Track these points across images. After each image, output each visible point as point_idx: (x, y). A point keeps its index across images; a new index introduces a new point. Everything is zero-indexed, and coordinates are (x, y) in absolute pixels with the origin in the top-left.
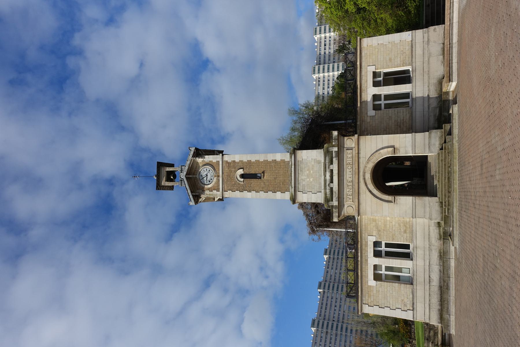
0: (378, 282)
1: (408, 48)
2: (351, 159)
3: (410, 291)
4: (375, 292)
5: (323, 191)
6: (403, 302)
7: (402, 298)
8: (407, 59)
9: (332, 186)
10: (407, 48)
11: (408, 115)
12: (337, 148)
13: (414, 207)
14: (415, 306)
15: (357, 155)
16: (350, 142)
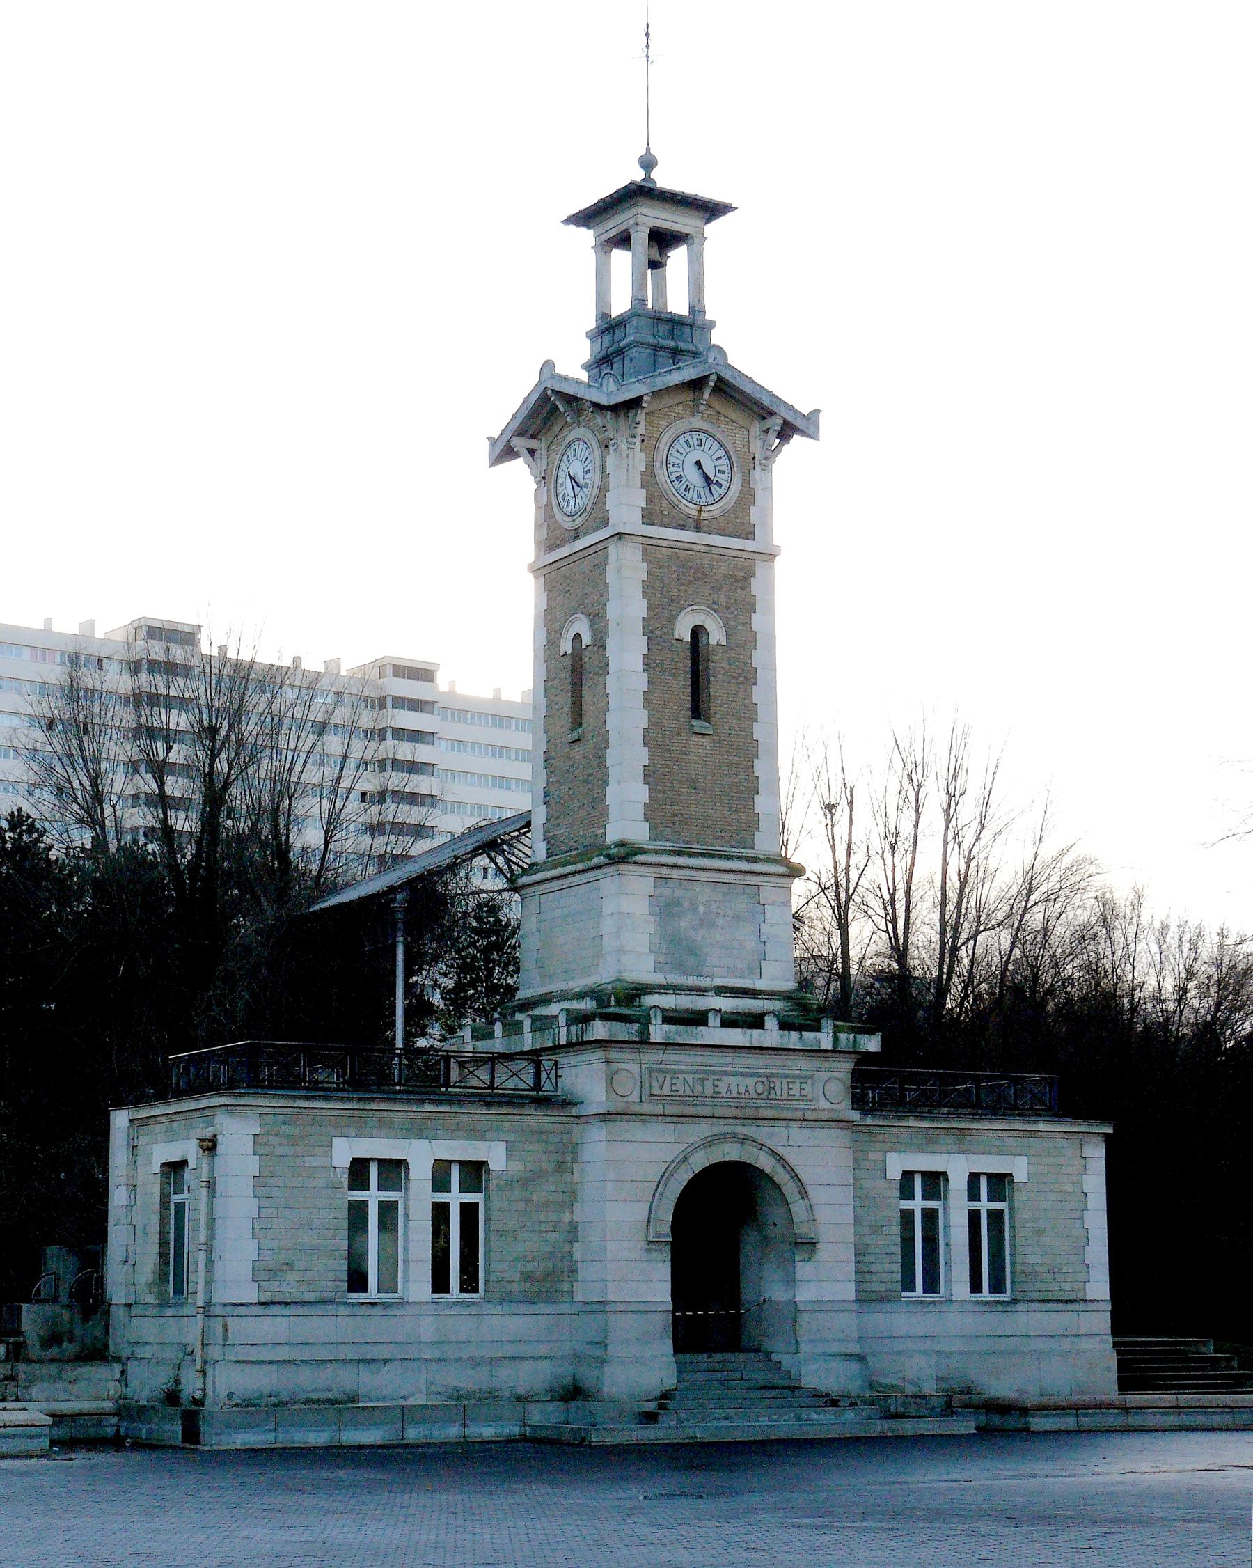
0: (346, 1176)
1: (1067, 1289)
2: (785, 1096)
3: (325, 1294)
4: (309, 1162)
6: (284, 1268)
7: (297, 1265)
8: (1039, 1286)
9: (711, 1023)
10: (1067, 1286)
11: (882, 1288)
12: (830, 1047)
13: (641, 1309)
14: (274, 1310)
15: (799, 1115)
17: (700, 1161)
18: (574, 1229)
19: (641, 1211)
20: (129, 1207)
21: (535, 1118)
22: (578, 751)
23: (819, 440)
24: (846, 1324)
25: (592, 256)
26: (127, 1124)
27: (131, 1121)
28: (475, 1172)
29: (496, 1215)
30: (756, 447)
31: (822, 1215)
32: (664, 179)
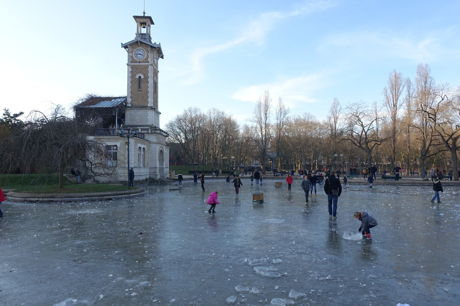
22: (139, 92)
26: (94, 138)
32: (146, 15)
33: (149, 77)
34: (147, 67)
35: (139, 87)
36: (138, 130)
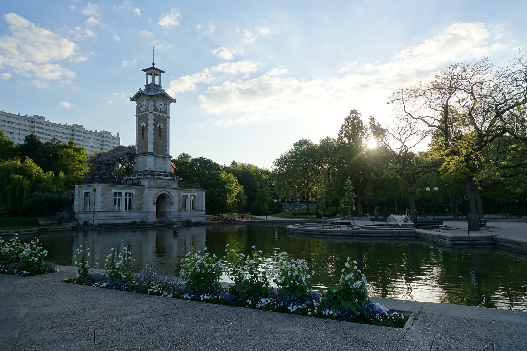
4: (109, 193)
5: (155, 170)
14: (104, 212)
16: (175, 185)
17: (160, 193)
18: (143, 202)
19: (152, 200)
20: (78, 199)
21: (139, 187)
22: (143, 140)
23: (175, 103)
24: (177, 214)
25: (145, 75)
27: (79, 187)
28: (130, 194)
29: (133, 200)
30: (168, 103)
31: (174, 200)
32: (155, 66)
33: (149, 124)
34: (147, 116)
35: (143, 135)
36: (135, 176)
